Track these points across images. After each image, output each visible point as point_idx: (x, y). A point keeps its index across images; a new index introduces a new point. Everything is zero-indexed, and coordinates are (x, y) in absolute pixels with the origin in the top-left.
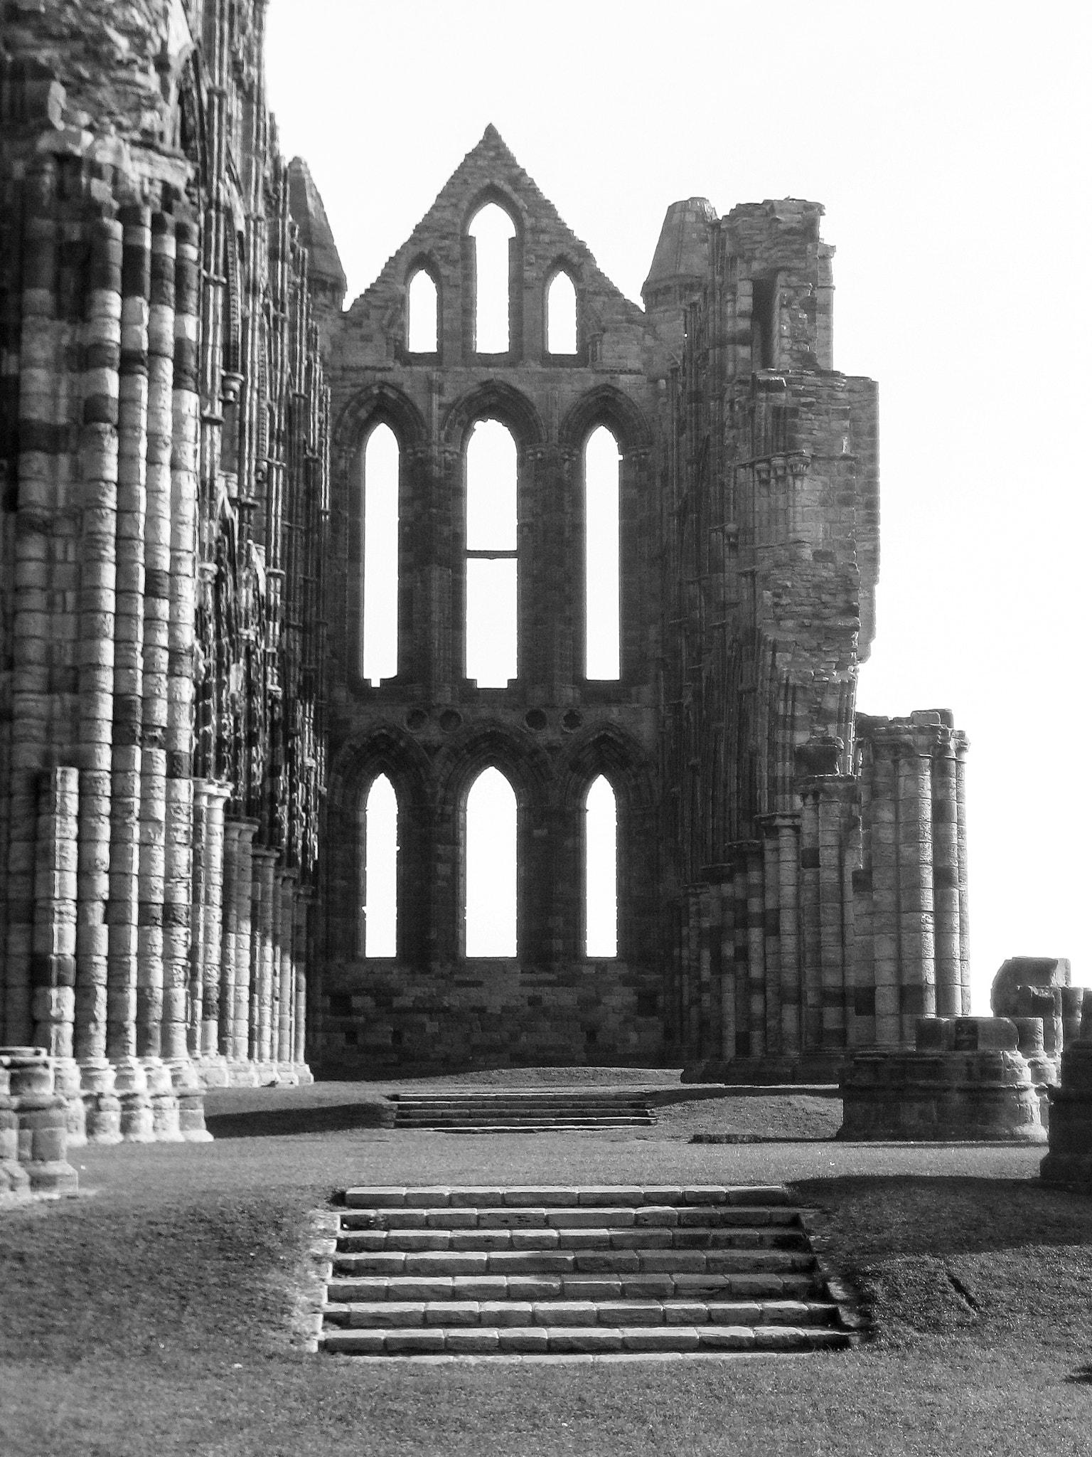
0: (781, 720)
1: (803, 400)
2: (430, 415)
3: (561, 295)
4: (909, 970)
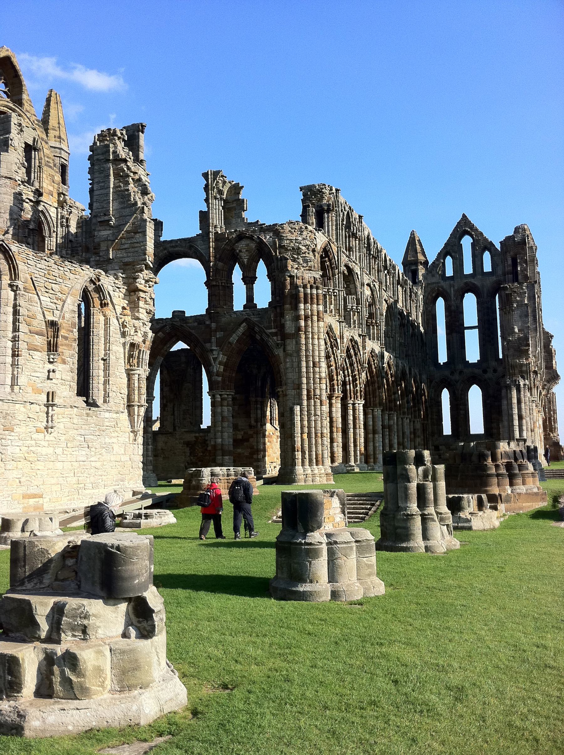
3: (487, 256)
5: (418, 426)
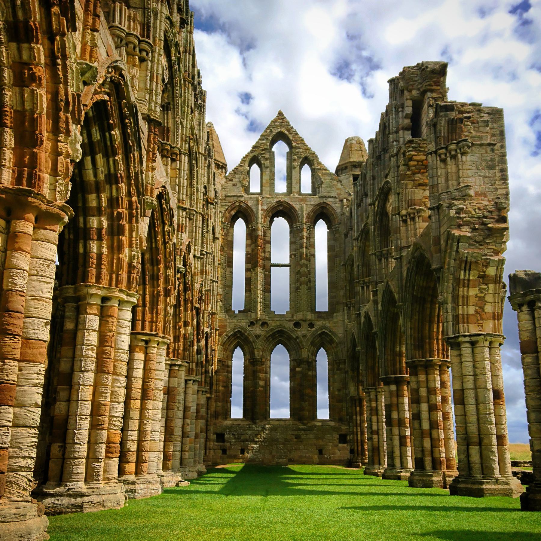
0: (462, 282)
1: (465, 115)
2: (258, 213)
5: (203, 401)
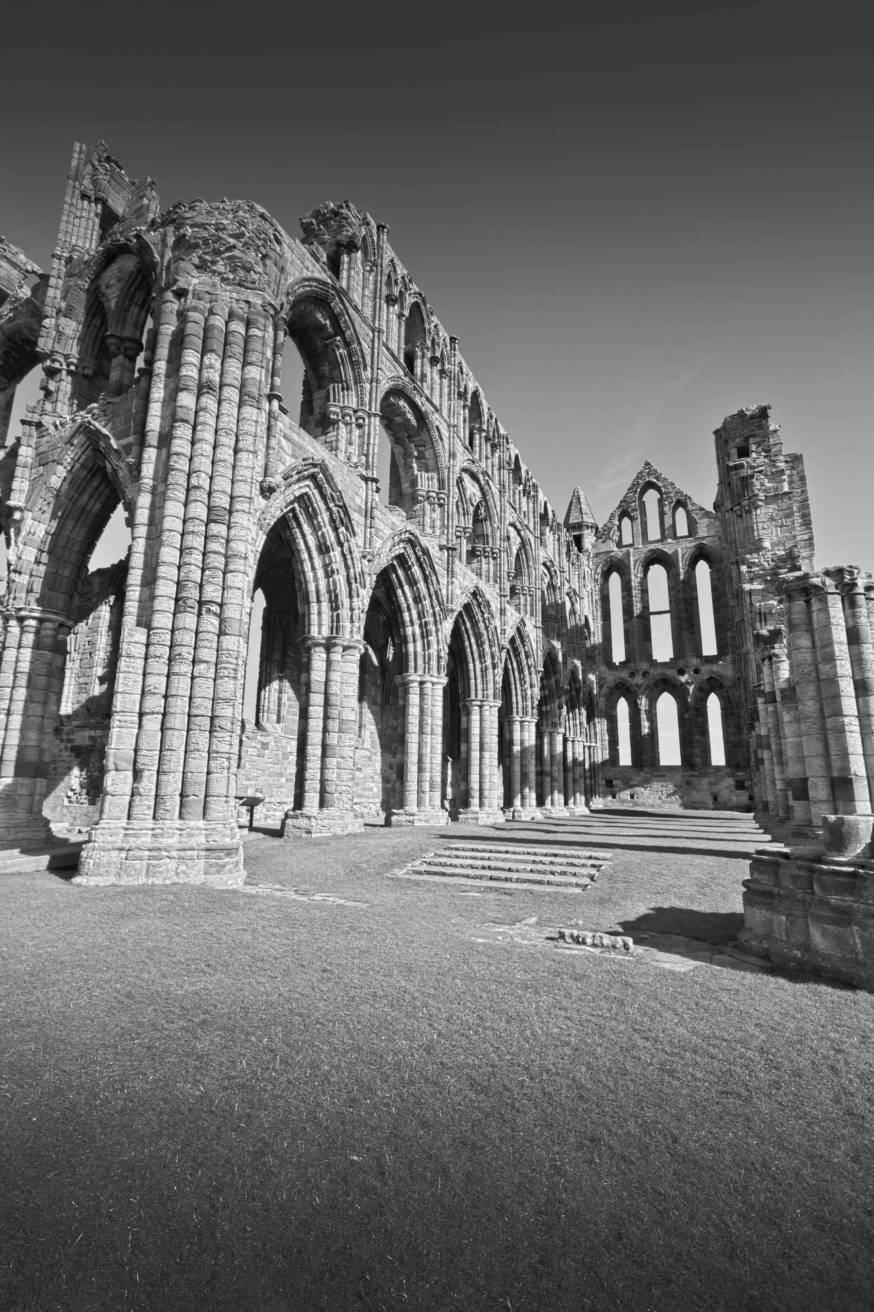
4: (836, 763)
